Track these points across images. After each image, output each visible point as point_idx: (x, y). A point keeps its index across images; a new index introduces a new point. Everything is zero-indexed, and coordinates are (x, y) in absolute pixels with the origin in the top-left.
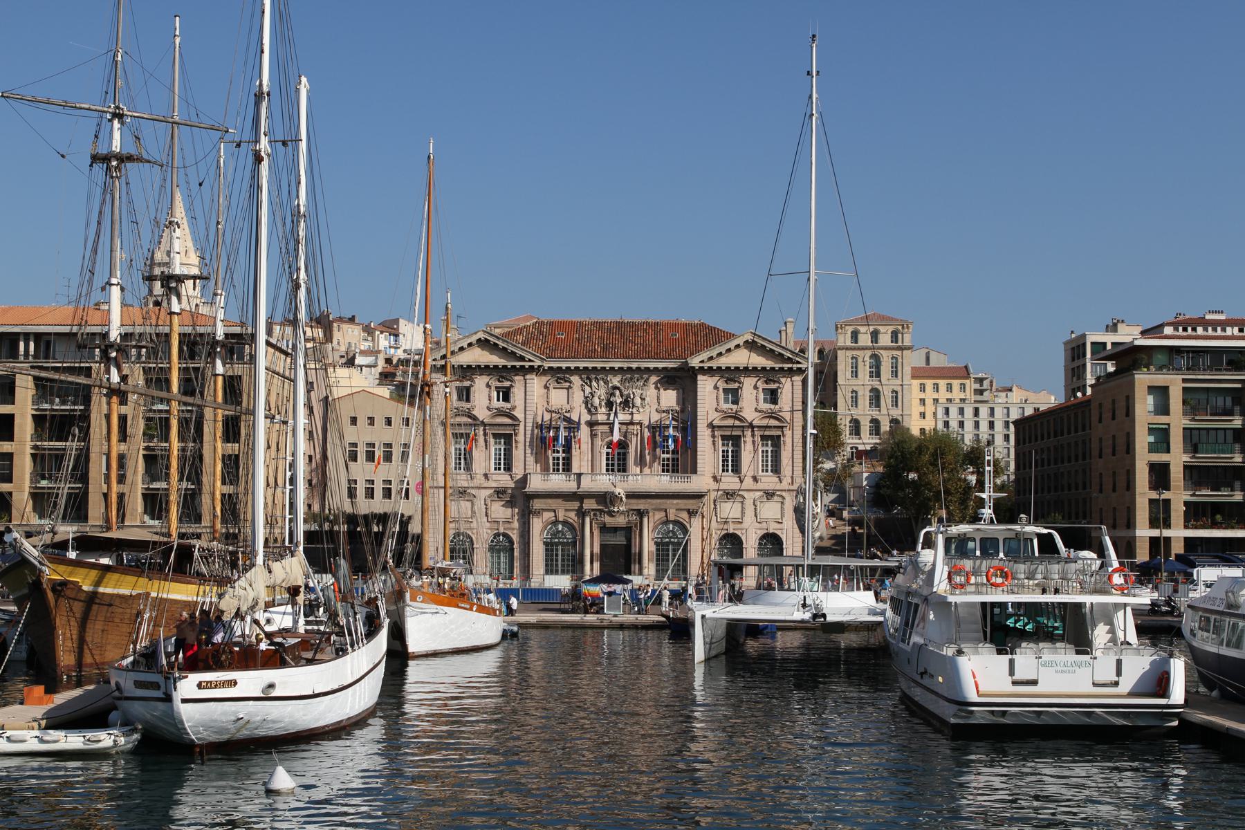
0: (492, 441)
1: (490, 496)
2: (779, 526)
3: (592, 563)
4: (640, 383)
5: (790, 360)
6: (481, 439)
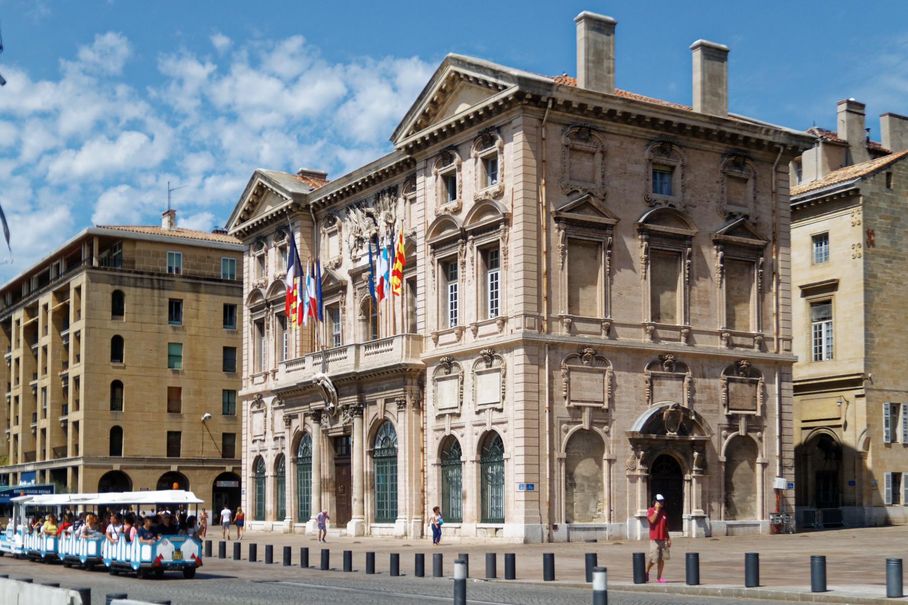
2: (497, 416)
4: (387, 199)
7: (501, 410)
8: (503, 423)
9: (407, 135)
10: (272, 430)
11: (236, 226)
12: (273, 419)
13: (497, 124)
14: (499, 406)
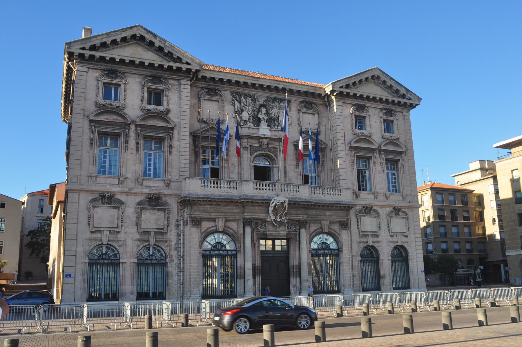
0: (142, 142)
1: (139, 203)
2: (405, 239)
3: (254, 277)
5: (403, 96)
6: (132, 142)
7: (407, 236)
8: (407, 242)
9: (342, 87)
10: (138, 224)
11: (84, 48)
12: (138, 218)
13: (395, 109)
14: (406, 234)
